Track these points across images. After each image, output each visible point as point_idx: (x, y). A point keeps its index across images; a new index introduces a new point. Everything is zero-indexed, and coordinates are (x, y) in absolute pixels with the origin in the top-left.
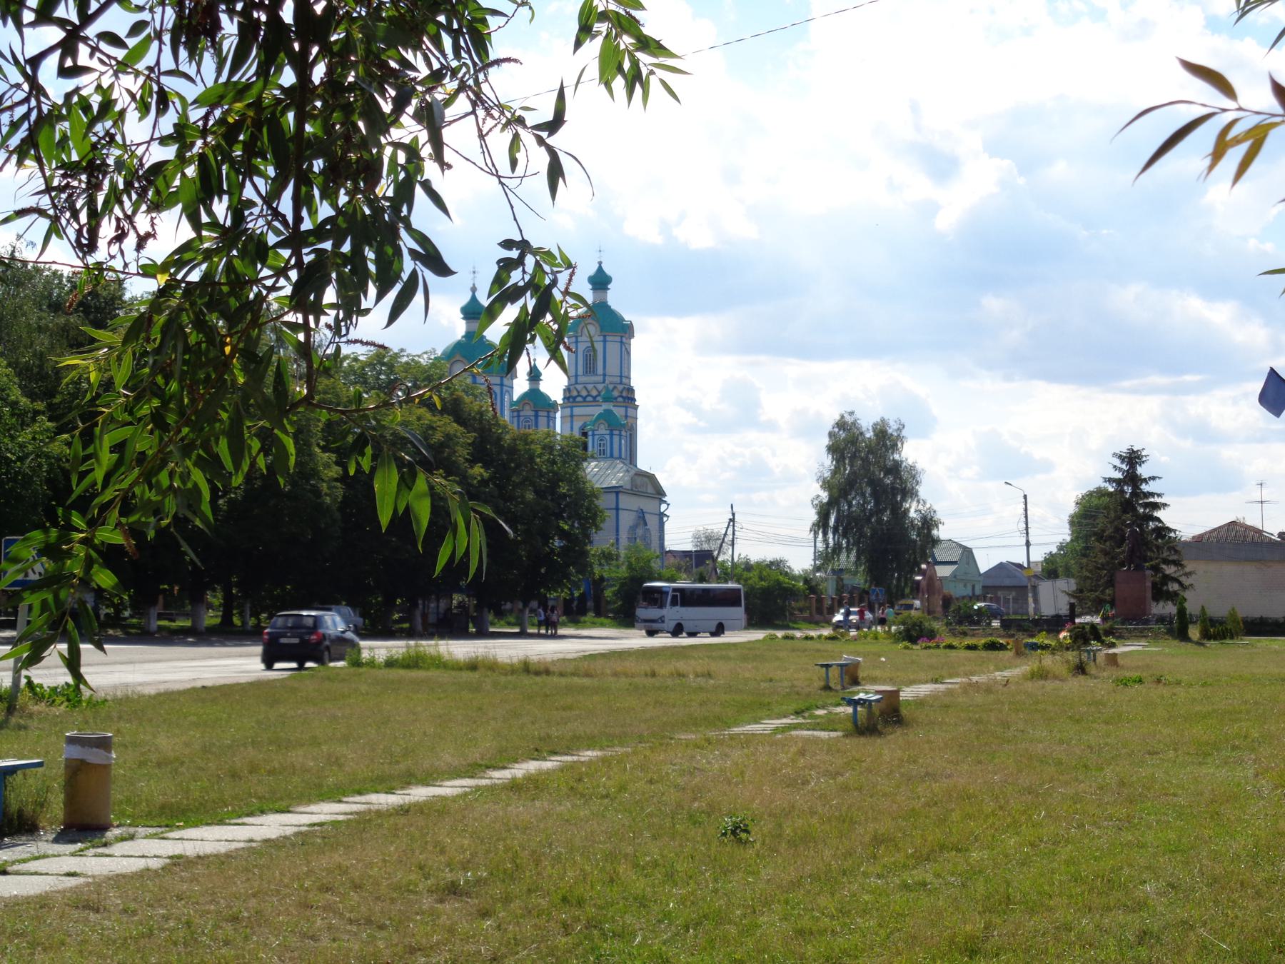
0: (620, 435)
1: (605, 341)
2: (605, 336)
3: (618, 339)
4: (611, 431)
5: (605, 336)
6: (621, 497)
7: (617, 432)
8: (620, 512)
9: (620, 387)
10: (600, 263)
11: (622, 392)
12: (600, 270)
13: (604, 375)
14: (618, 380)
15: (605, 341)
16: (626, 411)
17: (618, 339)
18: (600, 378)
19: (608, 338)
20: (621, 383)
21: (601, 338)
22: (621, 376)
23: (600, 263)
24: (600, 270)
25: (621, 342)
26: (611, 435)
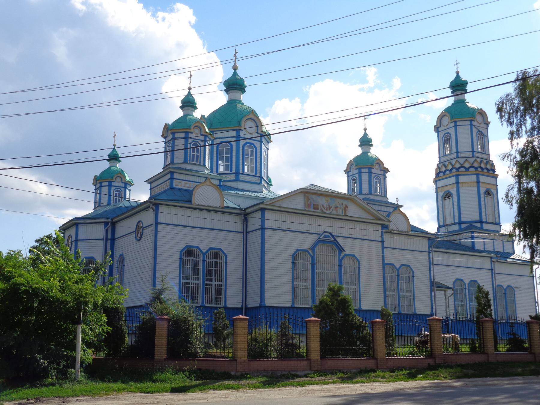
0: (370, 173)
1: (456, 126)
2: (455, 122)
3: (468, 123)
4: (360, 169)
5: (455, 122)
6: (268, 214)
7: (367, 170)
8: (267, 232)
9: (472, 160)
10: (458, 73)
11: (473, 164)
12: (458, 76)
13: (457, 152)
14: (470, 154)
15: (456, 126)
16: (478, 178)
17: (468, 123)
18: (454, 156)
19: (458, 123)
20: (473, 157)
21: (453, 124)
22: (473, 151)
23: (458, 73)
24: (458, 76)
25: (471, 125)
26: (360, 173)
